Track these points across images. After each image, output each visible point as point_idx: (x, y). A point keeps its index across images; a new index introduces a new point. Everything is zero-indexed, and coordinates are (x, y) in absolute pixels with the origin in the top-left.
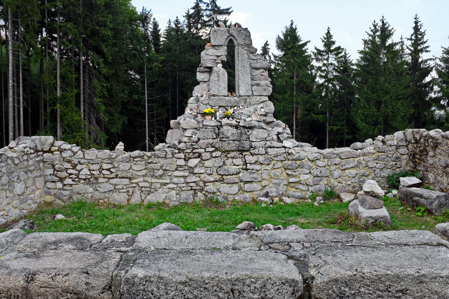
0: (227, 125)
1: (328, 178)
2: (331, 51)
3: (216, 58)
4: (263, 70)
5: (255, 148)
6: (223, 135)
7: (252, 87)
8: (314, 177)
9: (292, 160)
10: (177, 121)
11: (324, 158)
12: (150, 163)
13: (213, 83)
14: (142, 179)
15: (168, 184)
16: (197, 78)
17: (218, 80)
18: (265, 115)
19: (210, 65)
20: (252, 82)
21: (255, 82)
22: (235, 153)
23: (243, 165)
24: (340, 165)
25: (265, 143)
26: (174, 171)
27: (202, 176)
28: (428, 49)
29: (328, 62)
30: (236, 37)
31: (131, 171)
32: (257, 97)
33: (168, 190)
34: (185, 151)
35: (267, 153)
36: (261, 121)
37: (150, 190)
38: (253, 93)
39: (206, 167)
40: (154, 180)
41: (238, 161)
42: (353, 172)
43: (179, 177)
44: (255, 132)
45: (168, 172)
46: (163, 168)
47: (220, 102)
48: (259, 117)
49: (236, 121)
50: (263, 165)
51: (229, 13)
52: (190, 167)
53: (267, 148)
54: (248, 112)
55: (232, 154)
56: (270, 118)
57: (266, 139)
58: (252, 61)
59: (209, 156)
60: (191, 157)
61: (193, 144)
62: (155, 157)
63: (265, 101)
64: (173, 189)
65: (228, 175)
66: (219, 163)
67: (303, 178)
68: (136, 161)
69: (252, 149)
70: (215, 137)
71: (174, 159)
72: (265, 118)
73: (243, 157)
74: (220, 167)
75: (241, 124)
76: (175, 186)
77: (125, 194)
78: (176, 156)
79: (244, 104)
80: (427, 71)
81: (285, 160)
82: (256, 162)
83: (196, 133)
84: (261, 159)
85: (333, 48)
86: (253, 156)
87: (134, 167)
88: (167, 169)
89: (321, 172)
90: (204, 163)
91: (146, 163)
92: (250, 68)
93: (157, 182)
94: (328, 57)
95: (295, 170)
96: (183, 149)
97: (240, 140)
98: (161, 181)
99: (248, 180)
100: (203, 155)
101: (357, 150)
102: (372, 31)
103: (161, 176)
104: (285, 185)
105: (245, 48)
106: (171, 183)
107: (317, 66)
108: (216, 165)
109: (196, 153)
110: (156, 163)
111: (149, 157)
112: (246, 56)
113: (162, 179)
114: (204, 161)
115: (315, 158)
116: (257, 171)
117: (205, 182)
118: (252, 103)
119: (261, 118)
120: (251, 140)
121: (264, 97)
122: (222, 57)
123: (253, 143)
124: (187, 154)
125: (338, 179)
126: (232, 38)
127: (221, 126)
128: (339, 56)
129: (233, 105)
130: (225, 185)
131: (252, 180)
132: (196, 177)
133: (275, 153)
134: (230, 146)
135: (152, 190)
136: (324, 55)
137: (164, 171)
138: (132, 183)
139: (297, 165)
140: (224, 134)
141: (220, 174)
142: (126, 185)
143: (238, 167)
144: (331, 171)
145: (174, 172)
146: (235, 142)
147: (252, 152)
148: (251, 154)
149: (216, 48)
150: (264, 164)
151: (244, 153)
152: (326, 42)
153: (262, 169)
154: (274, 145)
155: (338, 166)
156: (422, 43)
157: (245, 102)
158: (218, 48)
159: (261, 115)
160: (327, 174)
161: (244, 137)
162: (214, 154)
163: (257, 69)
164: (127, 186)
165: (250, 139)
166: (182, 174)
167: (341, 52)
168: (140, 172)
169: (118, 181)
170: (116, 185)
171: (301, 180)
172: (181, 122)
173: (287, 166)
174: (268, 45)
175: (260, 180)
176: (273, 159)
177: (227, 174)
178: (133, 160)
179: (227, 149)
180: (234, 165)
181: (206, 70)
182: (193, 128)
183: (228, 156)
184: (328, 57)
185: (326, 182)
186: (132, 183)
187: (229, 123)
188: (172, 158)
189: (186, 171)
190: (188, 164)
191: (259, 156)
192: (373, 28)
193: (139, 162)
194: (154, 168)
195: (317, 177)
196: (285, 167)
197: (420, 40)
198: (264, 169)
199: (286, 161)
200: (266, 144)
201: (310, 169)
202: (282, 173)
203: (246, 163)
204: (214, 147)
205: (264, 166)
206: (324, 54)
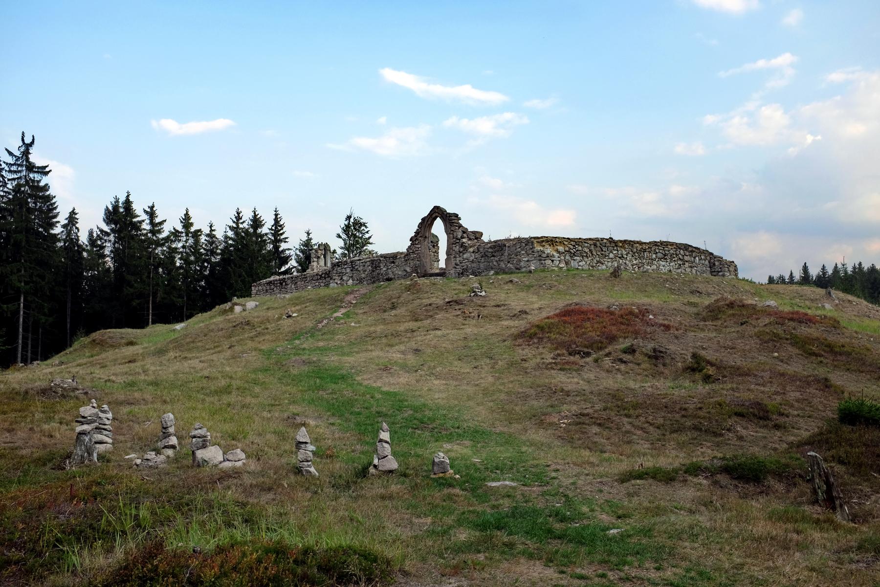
28: (287, 240)
51: (47, 173)
85: (193, 229)
102: (236, 218)
174: (76, 214)
192: (236, 215)
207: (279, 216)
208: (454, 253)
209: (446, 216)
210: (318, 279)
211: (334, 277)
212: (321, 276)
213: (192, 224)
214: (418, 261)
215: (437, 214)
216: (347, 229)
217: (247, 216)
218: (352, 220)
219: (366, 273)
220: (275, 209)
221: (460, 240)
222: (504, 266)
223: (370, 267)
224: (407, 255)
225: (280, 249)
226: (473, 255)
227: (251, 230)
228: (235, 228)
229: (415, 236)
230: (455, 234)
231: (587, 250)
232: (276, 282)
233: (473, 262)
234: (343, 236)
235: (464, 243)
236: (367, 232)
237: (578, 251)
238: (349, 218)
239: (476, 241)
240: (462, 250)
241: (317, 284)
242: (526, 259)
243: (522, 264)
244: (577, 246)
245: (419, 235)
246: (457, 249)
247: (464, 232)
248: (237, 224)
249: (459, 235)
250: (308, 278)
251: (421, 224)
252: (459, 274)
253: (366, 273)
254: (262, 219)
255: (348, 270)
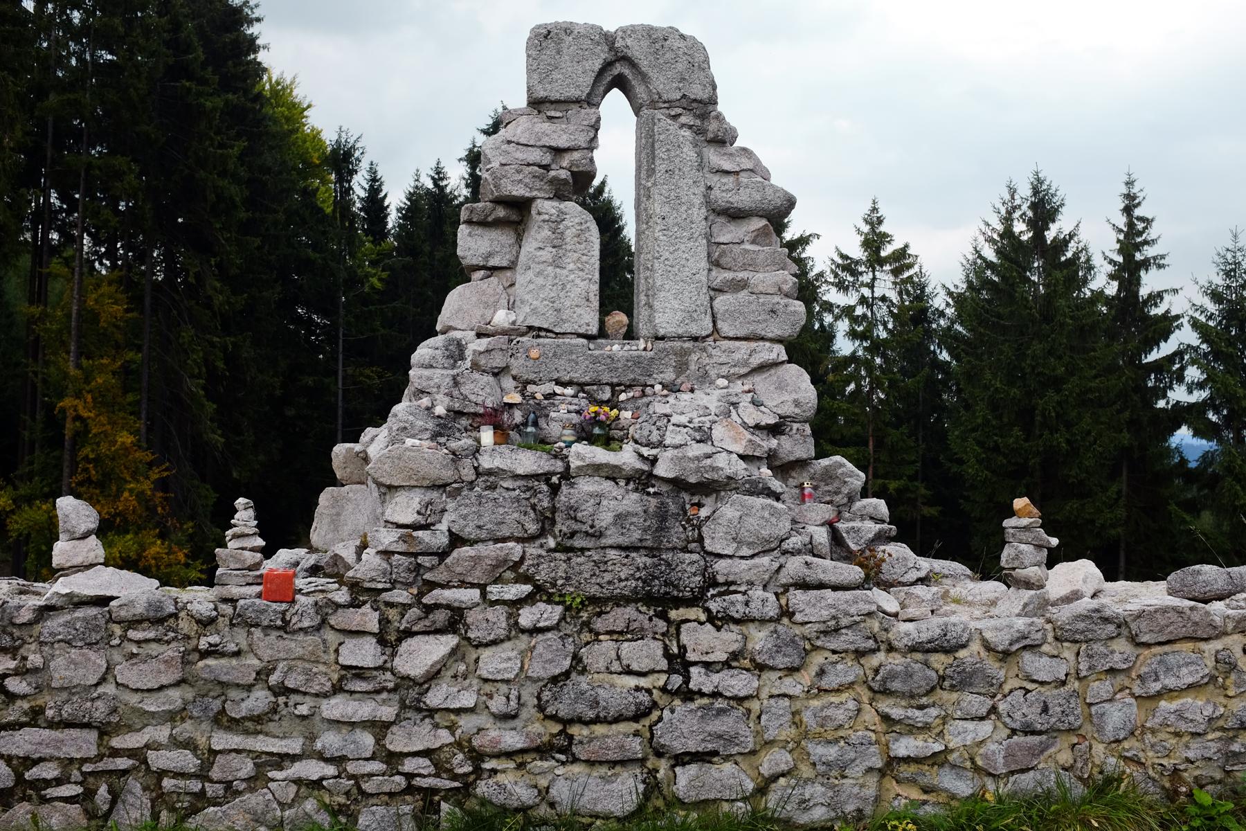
0: (596, 469)
1: (1075, 740)
2: (882, 262)
3: (547, 159)
4: (764, 222)
5: (729, 587)
6: (575, 519)
7: (712, 299)
8: (1014, 732)
9: (913, 649)
10: (357, 447)
11: (1056, 639)
12: (205, 654)
13: (530, 274)
14: (162, 733)
15: (294, 758)
16: (459, 252)
17: (556, 263)
18: (775, 430)
19: (519, 191)
20: (714, 273)
21: (729, 275)
22: (629, 611)
23: (670, 671)
24: (1134, 675)
25: (776, 565)
26: (325, 696)
27: (466, 724)
29: (873, 292)
30: (644, 64)
31: (109, 689)
32: (737, 343)
33: (293, 789)
34: (386, 596)
35: (787, 613)
36: (759, 458)
37: (203, 791)
38: (720, 324)
39: (486, 680)
40: (221, 740)
41: (645, 653)
42: (1198, 707)
43: (353, 725)
44: (729, 510)
45: (294, 698)
46: (274, 679)
47: (562, 363)
48: (750, 437)
49: (641, 456)
50: (766, 675)
52: (408, 678)
53: (786, 588)
54: (694, 414)
55: (618, 617)
56: (797, 445)
57: (785, 546)
58: (716, 178)
59: (504, 625)
60: (415, 629)
61: (425, 561)
62: (232, 625)
63: (776, 364)
64: (317, 784)
65: (597, 720)
66: (551, 661)
67: (962, 734)
68: (139, 643)
69: (712, 592)
70: (532, 528)
71: (331, 637)
72: (774, 443)
73: (673, 630)
74: (554, 680)
75: (661, 470)
76: (331, 770)
77: (75, 810)
78: (339, 619)
79: (673, 376)
81: (874, 651)
82: (735, 656)
83: (443, 511)
84: (760, 639)
86: (719, 629)
87: (127, 673)
88: (290, 684)
89: (1045, 709)
90: (477, 660)
91: (185, 654)
92: (704, 210)
93: (238, 751)
94: (874, 279)
95: (924, 700)
96: (373, 585)
97: (658, 549)
98: (262, 744)
99: (693, 746)
100: (471, 617)
101: (1206, 602)
103: (258, 719)
104: (870, 770)
105: (683, 119)
106: (309, 757)
107: (842, 305)
108: (537, 669)
109: (437, 606)
110: (237, 654)
111: (206, 623)
112: (689, 153)
113: (267, 734)
114: (477, 647)
115: (1018, 640)
116: (740, 700)
117: (477, 757)
118: (713, 373)
119: (757, 440)
120: (709, 548)
121: (768, 344)
122: (576, 155)
123: (721, 566)
124: (392, 614)
125: (1126, 745)
126: (627, 71)
127: (566, 475)
128: (906, 275)
129: (625, 380)
130: (576, 769)
131: (710, 746)
132: (436, 726)
133: (825, 614)
134: (608, 577)
135: (211, 790)
136: (861, 274)
137: (276, 695)
138: (116, 753)
139: (934, 675)
140: (579, 515)
141: (554, 718)
142: (84, 761)
143: (643, 682)
144: (1090, 705)
145: (325, 701)
146: (634, 555)
147: (714, 606)
148: (711, 619)
149: (553, 114)
150: (773, 669)
151: (673, 614)
152: (866, 234)
153: (764, 694)
154: (821, 576)
155: (1121, 680)
156: (1146, 242)
157: (681, 367)
158: (558, 114)
159: (757, 427)
160: (1072, 718)
161: (677, 533)
162: (527, 617)
163: (736, 215)
164: (87, 768)
165: (707, 542)
166: (365, 710)
167: (910, 266)
168: (156, 695)
169: (37, 739)
170: (30, 762)
171: (951, 746)
172: (373, 451)
173: (884, 680)
175: (751, 746)
176: (819, 643)
177: (591, 714)
178: (124, 638)
179: (594, 590)
180: (628, 672)
181: (501, 212)
182: (426, 483)
183: (599, 624)
184: (874, 279)
185: (1065, 757)
186: (116, 753)
187: (607, 465)
188: (318, 629)
189: (384, 695)
190: (397, 660)
191: (752, 629)
193: (154, 645)
194: (224, 678)
195: (1026, 733)
196: (876, 686)
197: (1140, 233)
198: (776, 692)
199: (880, 657)
200: (784, 572)
201: (994, 696)
202: (859, 710)
203: (678, 662)
204: (526, 579)
205: (774, 675)
206: (860, 269)
213: (884, 238)
217: (1025, 191)
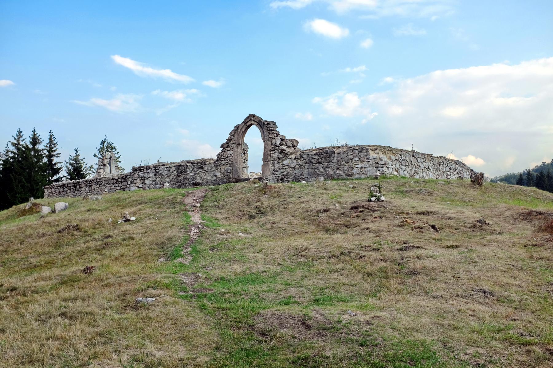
28: (59, 155)
80: (57, 171)
102: (17, 136)
192: (18, 134)
197: (53, 148)
207: (53, 137)
208: (272, 159)
209: (264, 123)
210: (113, 183)
211: (135, 181)
212: (117, 180)
214: (230, 166)
215: (253, 122)
216: (101, 151)
218: (105, 144)
219: (171, 177)
220: (50, 131)
221: (279, 147)
222: (332, 173)
223: (175, 172)
224: (218, 162)
225: (53, 162)
226: (295, 161)
227: (31, 146)
228: (16, 144)
229: (227, 143)
230: (274, 141)
231: (409, 160)
232: (69, 185)
233: (294, 168)
234: (98, 156)
235: (284, 149)
236: (117, 153)
237: (403, 160)
238: (103, 142)
239: (293, 148)
240: (281, 156)
241: (113, 187)
242: (360, 166)
243: (355, 171)
244: (402, 156)
245: (232, 142)
246: (276, 155)
247: (282, 140)
248: (18, 141)
249: (278, 142)
250: (104, 183)
251: (234, 131)
252: (278, 180)
253: (171, 177)
254: (40, 137)
255: (151, 175)
